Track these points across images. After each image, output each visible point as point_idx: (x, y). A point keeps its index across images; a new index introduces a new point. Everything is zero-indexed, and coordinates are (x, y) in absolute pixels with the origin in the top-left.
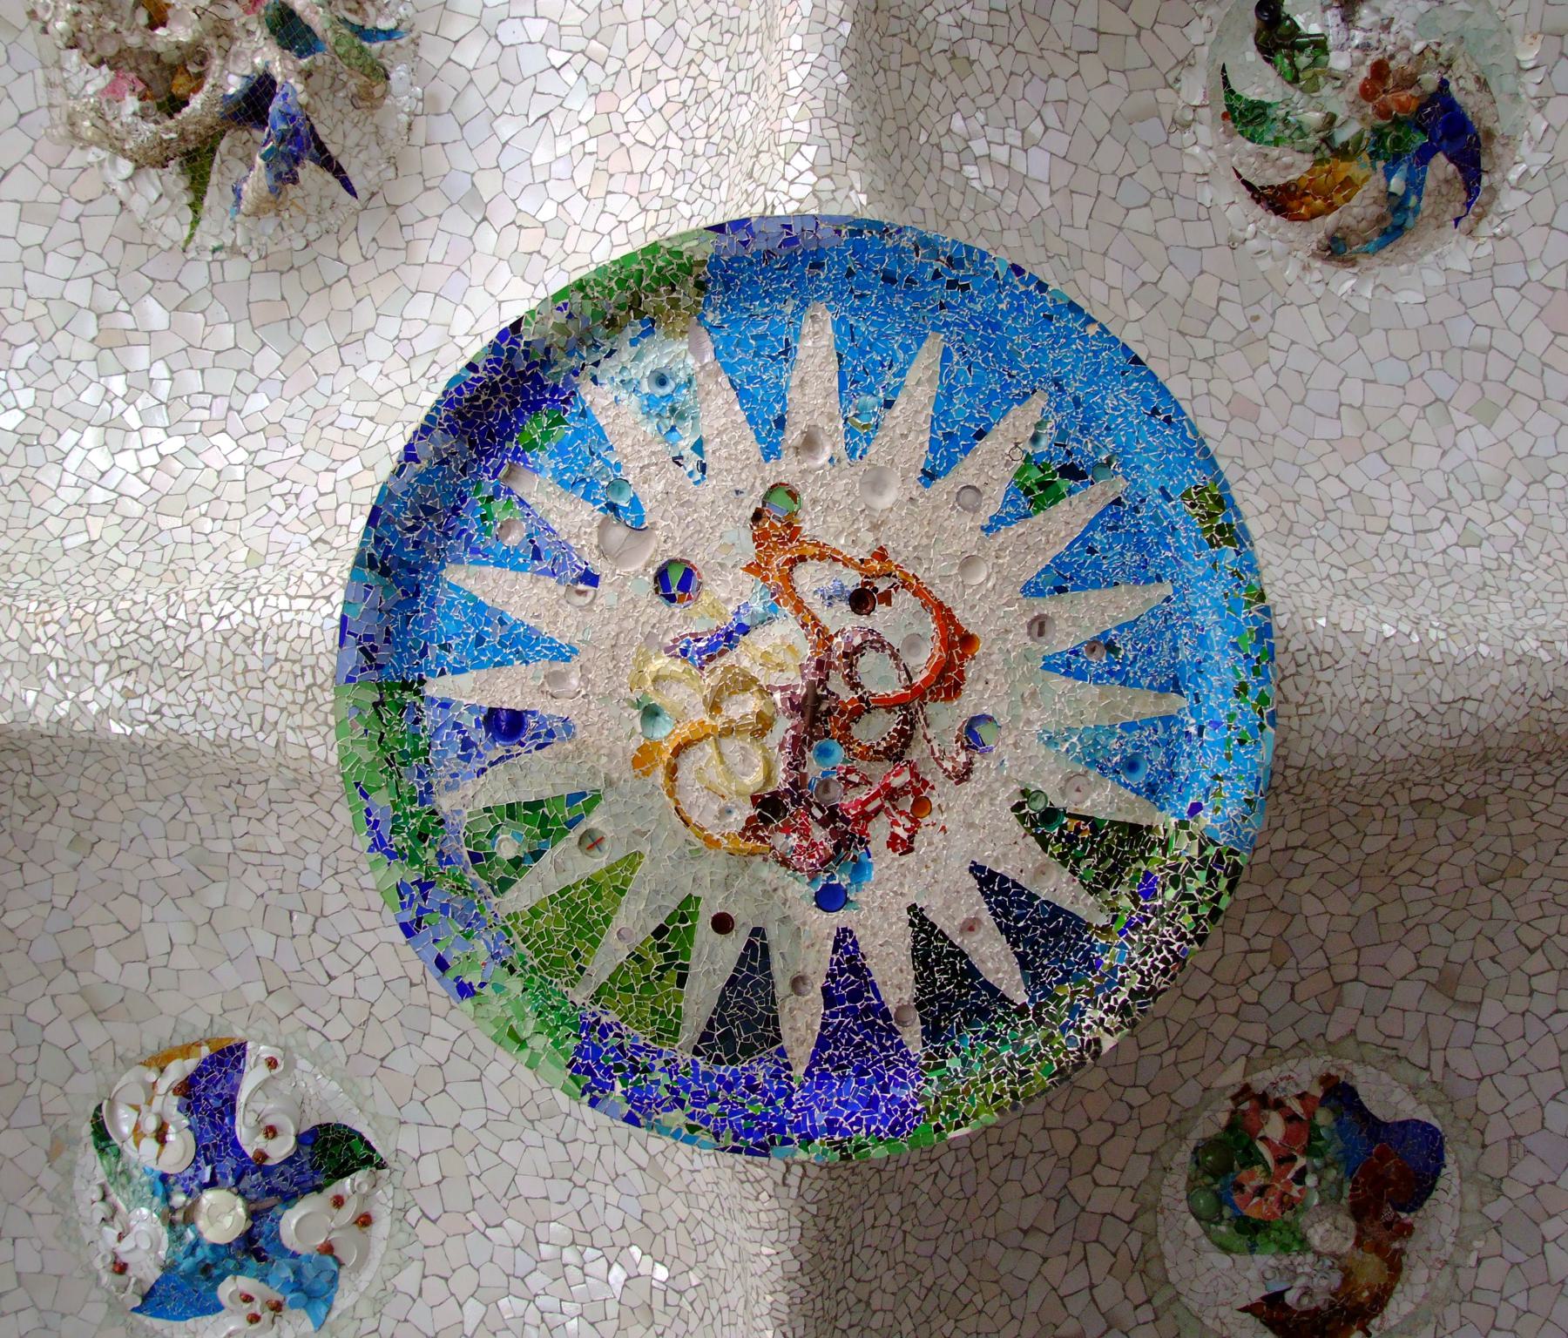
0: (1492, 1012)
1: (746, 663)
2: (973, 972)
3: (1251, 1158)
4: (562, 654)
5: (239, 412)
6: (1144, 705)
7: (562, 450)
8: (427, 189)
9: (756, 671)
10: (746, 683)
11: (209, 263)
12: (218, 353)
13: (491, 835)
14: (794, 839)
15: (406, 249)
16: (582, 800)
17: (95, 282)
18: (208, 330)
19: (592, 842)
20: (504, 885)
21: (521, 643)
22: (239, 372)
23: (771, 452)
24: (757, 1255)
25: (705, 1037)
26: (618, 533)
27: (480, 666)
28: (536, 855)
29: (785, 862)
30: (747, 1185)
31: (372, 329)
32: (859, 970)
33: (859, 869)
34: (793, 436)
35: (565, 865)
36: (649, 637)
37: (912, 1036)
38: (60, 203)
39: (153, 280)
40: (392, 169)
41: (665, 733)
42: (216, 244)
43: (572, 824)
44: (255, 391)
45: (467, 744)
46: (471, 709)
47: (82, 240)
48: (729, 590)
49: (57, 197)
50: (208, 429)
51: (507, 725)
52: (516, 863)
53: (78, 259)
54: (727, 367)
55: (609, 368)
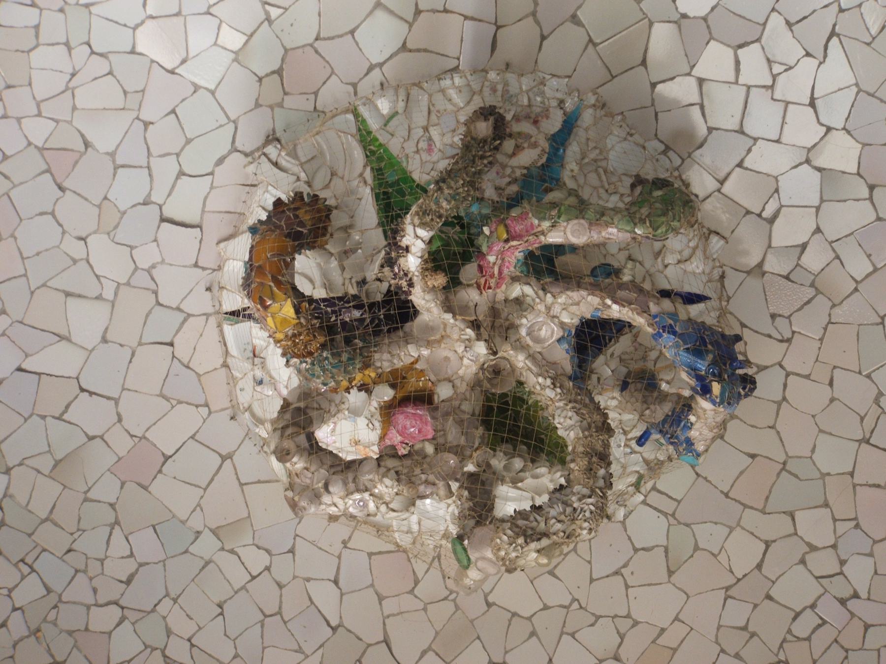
5: (856, 595)
8: (772, 221)
11: (644, 502)
12: (759, 566)
15: (818, 292)
17: (573, 635)
18: (722, 558)
22: (803, 562)
31: (880, 394)
38: (457, 608)
39: (616, 573)
40: (714, 239)
42: (633, 479)
44: (843, 563)
47: (514, 614)
49: (449, 607)
50: (851, 639)
53: (533, 634)
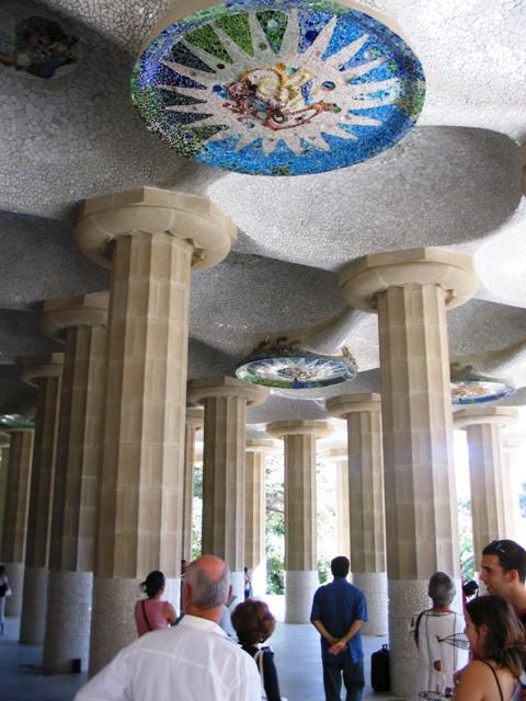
0: (90, 103)
1: (297, 98)
2: (180, 104)
3: (52, 40)
4: (324, 57)
6: (238, 147)
7: (383, 71)
9: (293, 100)
10: (290, 98)
13: (277, 21)
14: (239, 88)
16: (277, 49)
19: (262, 46)
20: (259, 18)
21: (334, 48)
23: (350, 111)
24: (88, 6)
25: (184, 47)
26: (350, 77)
27: (334, 35)
28: (265, 31)
29: (233, 84)
30: (119, 19)
32: (192, 87)
33: (223, 96)
34: (351, 115)
35: (258, 35)
36: (316, 77)
37: (165, 87)
41: (285, 74)
43: (271, 44)
45: (311, 24)
46: (321, 29)
48: (319, 96)
51: (311, 36)
52: (266, 24)
54: (378, 108)
55: (398, 86)
